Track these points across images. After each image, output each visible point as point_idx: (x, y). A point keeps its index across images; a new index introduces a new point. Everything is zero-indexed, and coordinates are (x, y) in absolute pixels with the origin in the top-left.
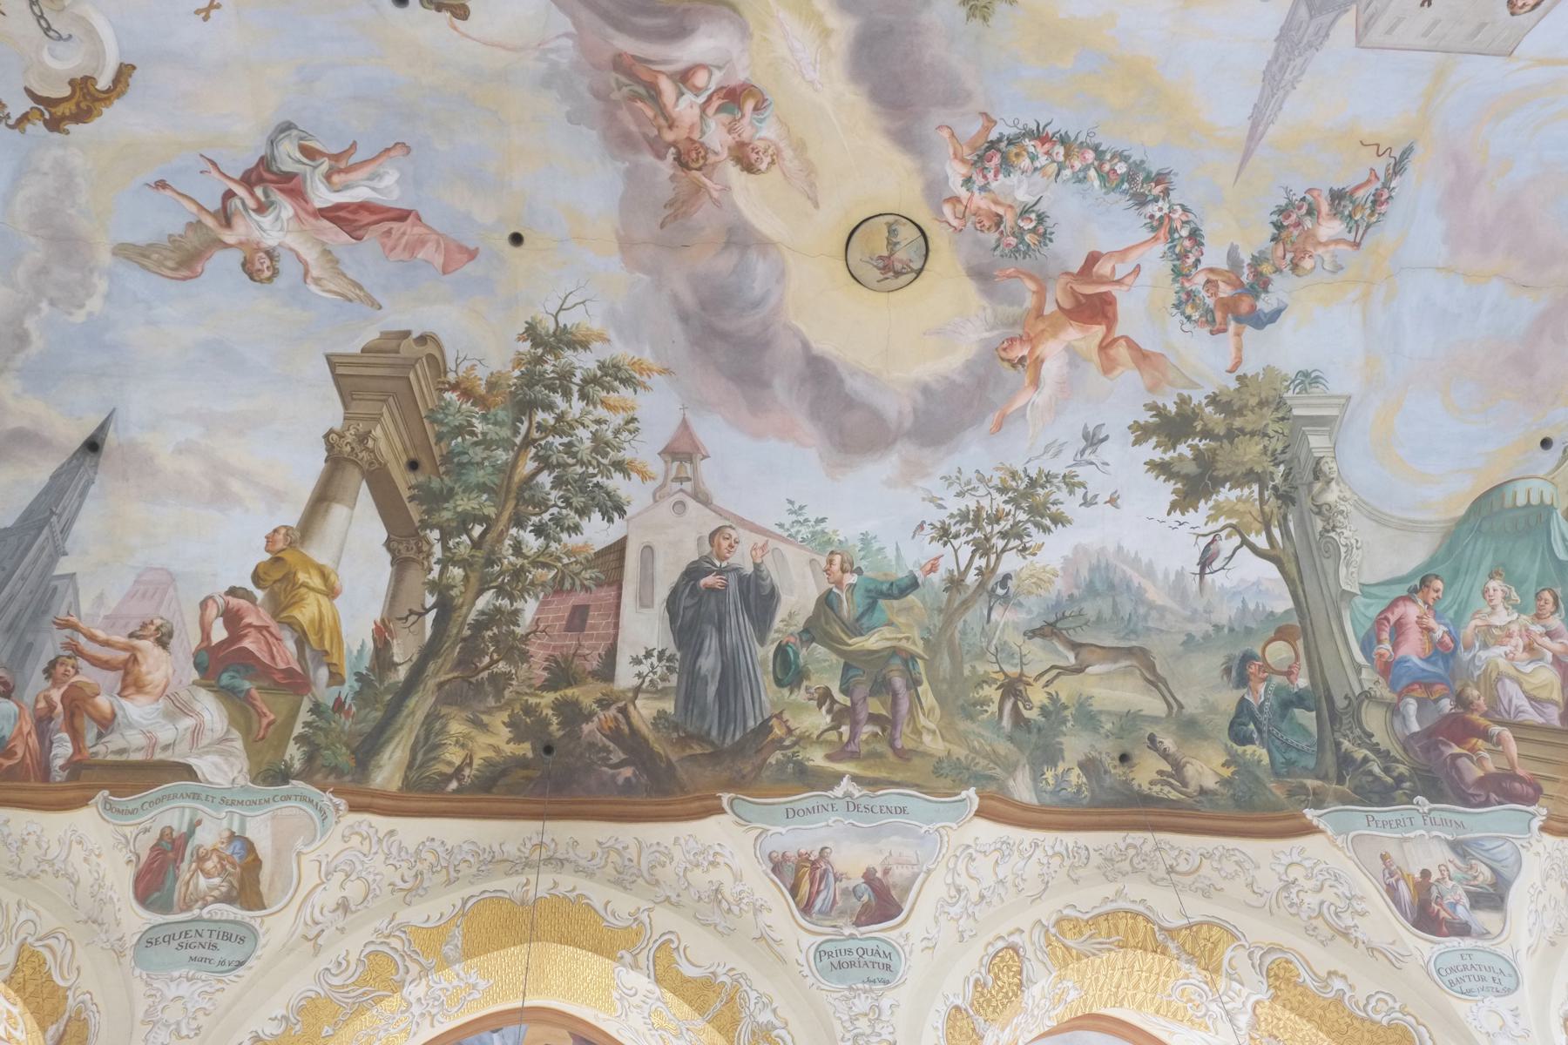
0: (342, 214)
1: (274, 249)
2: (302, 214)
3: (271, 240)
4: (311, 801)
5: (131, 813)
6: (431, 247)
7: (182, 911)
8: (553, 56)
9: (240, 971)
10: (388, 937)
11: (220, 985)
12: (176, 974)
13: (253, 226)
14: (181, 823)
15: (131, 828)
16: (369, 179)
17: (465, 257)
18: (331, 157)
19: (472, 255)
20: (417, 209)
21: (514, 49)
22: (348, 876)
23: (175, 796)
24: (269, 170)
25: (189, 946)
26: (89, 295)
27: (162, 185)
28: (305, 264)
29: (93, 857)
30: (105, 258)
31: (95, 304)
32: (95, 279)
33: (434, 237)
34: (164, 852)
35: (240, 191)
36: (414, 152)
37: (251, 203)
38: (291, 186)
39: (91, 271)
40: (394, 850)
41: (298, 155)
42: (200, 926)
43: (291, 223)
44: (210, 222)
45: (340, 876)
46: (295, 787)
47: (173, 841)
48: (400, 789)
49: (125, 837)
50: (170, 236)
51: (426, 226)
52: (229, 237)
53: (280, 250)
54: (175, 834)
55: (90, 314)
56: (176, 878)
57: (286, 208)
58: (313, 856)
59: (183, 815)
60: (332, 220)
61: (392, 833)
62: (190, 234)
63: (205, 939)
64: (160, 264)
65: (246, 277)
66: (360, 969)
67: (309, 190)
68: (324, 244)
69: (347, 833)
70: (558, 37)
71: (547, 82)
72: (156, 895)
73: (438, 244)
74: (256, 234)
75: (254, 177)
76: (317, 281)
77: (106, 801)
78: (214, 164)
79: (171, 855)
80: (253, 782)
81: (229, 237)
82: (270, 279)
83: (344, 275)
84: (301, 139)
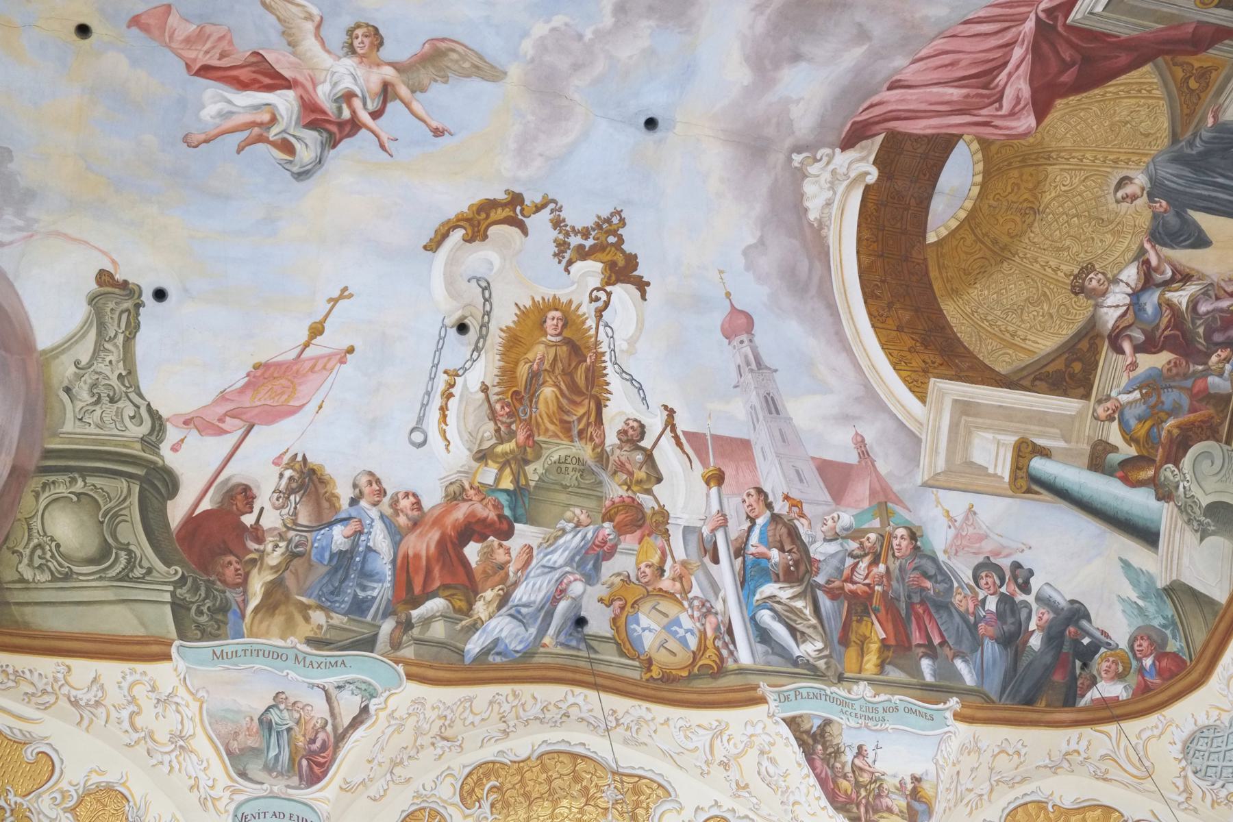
0: (267, 81)
1: (346, 55)
2: (309, 86)
3: (349, 63)
6: (180, 35)
8: (20, 223)
13: (361, 81)
16: (232, 113)
17: (143, 20)
18: (267, 141)
19: (135, 21)
20: (187, 76)
21: (58, 234)
24: (331, 133)
26: (542, 38)
27: (438, 133)
28: (317, 35)
30: (515, 71)
31: (540, 29)
32: (531, 53)
33: (174, 45)
35: (364, 117)
36: (181, 135)
37: (357, 103)
38: (313, 117)
39: (532, 60)
41: (298, 145)
43: (322, 79)
44: (403, 91)
50: (446, 82)
51: (180, 56)
52: (389, 73)
53: (341, 53)
55: (547, 22)
57: (323, 94)
60: (278, 76)
62: (426, 81)
64: (464, 58)
65: (382, 32)
67: (296, 109)
68: (294, 54)
70: (11, 243)
71: (30, 195)
73: (171, 37)
74: (361, 72)
75: (347, 129)
76: (309, 17)
78: (382, 147)
81: (389, 73)
82: (358, 26)
83: (279, 19)
84: (291, 162)
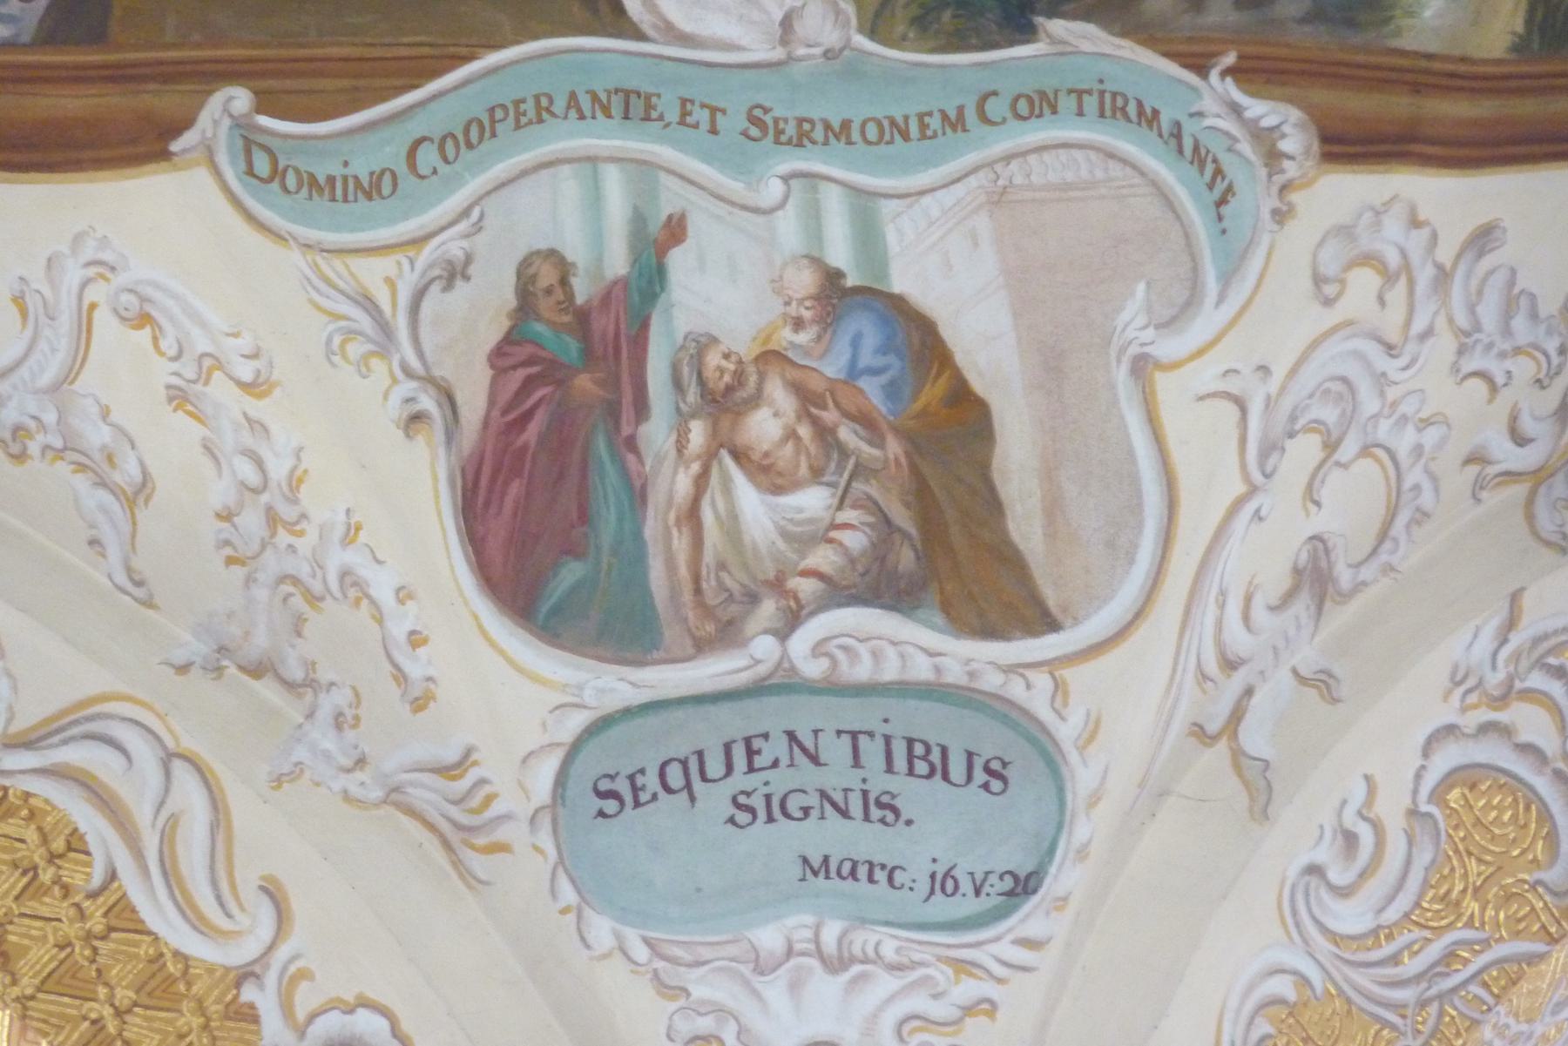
4: (1149, 118)
5: (372, 189)
7: (702, 647)
9: (1031, 919)
10: (1502, 700)
11: (968, 989)
12: (769, 938)
14: (597, 237)
15: (383, 266)
22: (1331, 446)
23: (543, 110)
25: (778, 809)
29: (220, 391)
34: (550, 372)
40: (1489, 313)
42: (805, 716)
45: (1304, 451)
46: (1065, 51)
47: (583, 318)
48: (1520, 47)
49: (367, 303)
54: (583, 290)
56: (638, 496)
58: (1206, 374)
59: (594, 199)
61: (1483, 238)
63: (837, 774)
66: (1424, 857)
69: (1330, 264)
72: (571, 573)
77: (249, 142)
79: (584, 382)
80: (872, 33)
